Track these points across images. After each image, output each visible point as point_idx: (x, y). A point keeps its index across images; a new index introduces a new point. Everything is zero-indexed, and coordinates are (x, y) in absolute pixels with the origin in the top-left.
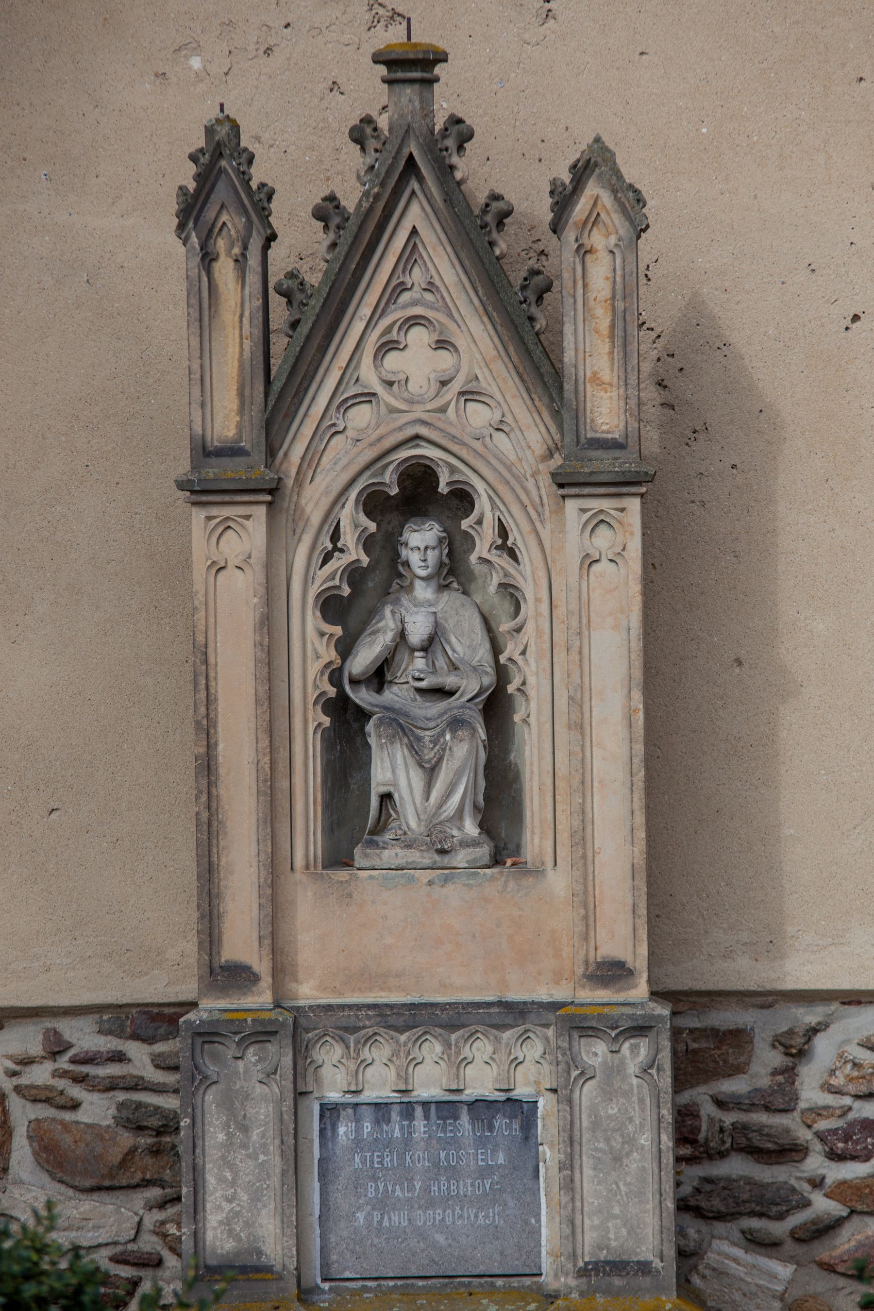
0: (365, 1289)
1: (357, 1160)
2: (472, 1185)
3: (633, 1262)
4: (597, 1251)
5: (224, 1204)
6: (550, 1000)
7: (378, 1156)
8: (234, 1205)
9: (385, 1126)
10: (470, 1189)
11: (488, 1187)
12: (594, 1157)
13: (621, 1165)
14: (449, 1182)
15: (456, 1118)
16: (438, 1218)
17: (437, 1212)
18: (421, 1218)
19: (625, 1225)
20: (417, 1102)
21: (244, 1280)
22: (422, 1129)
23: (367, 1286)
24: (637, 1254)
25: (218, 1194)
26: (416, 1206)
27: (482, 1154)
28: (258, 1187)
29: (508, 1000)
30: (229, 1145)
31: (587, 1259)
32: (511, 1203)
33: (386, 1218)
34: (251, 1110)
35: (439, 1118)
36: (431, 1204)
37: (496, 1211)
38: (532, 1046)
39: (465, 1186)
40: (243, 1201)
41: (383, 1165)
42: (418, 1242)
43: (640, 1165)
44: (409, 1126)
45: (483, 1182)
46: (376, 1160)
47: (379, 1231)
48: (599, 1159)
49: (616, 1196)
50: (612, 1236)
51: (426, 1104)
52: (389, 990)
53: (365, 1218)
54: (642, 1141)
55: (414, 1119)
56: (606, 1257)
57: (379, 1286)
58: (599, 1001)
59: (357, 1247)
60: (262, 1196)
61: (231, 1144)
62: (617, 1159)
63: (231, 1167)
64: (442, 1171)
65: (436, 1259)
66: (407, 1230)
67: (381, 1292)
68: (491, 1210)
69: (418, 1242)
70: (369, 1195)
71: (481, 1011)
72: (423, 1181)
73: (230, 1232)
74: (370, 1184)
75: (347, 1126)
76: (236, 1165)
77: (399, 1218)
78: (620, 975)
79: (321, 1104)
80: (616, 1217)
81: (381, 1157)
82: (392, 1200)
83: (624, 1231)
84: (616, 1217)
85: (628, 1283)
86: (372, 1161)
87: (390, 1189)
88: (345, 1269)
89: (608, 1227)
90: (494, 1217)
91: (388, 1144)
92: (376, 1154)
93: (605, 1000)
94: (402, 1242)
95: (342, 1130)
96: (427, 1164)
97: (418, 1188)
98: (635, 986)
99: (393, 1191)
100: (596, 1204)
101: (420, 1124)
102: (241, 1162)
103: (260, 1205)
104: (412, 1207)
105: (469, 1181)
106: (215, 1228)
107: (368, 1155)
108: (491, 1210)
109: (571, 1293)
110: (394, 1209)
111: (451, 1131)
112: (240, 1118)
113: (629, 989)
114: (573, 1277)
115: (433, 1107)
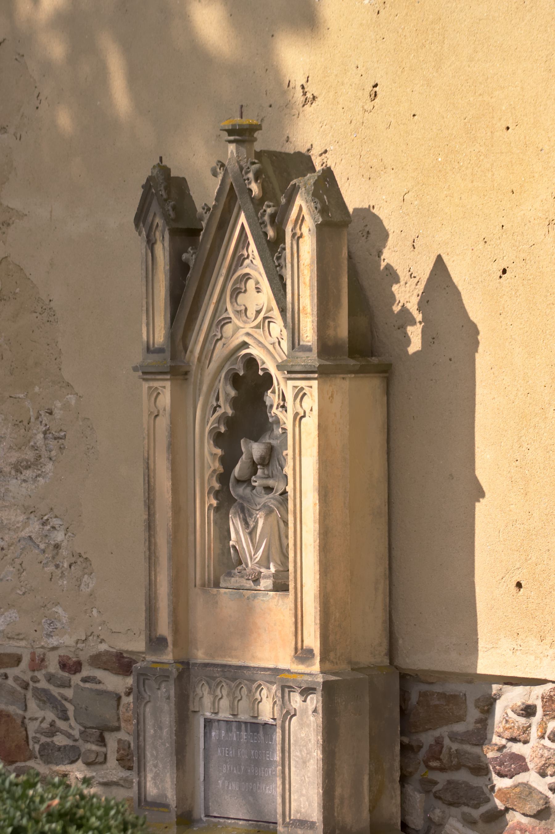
1: (219, 751)
3: (309, 821)
13: (306, 766)
14: (255, 768)
22: (245, 737)
50: (302, 806)
51: (246, 723)
56: (300, 817)
58: (300, 671)
86: (225, 753)
89: (300, 801)
93: (303, 671)
97: (242, 769)
98: (314, 664)
99: (233, 770)
111: (256, 740)
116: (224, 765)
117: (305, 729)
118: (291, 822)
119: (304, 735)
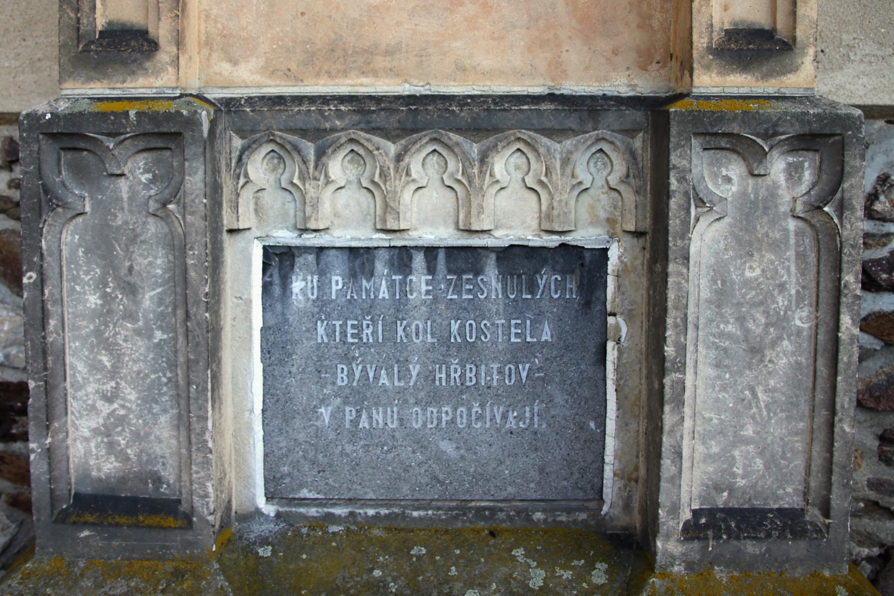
0: (331, 518)
1: (321, 330)
2: (500, 372)
3: (771, 510)
4: (713, 492)
5: (100, 404)
6: (631, 94)
7: (353, 326)
8: (116, 406)
9: (364, 282)
10: (496, 377)
11: (524, 375)
12: (717, 348)
13: (762, 361)
14: (463, 367)
15: (478, 272)
16: (444, 418)
17: (444, 409)
18: (418, 418)
19: (761, 454)
20: (416, 248)
21: (129, 526)
22: (424, 288)
23: (333, 515)
24: (777, 498)
25: (91, 388)
26: (412, 401)
27: (517, 326)
28: (153, 381)
29: (565, 92)
30: (105, 313)
31: (695, 506)
32: (559, 399)
33: (364, 416)
34: (140, 260)
35: (450, 271)
36: (435, 397)
37: (536, 410)
38: (604, 164)
39: (489, 373)
40: (130, 401)
41: (361, 339)
42: (414, 452)
43: (792, 359)
44: (403, 283)
45: (517, 368)
46: (350, 331)
47: (354, 434)
48: (725, 350)
49: (750, 408)
51: (430, 251)
52: (375, 74)
53: (332, 415)
54: (798, 323)
55: (410, 273)
56: (726, 502)
57: (352, 514)
58: (735, 91)
59: (320, 456)
60: (161, 395)
61: (110, 312)
62: (756, 351)
63: (110, 347)
64: (453, 351)
65: (441, 477)
66: (397, 434)
67: (355, 523)
68: (527, 409)
69: (414, 452)
70: (339, 383)
71: (526, 107)
72: (424, 365)
73: (111, 447)
74: (340, 366)
75: (305, 280)
76: (117, 344)
77: (385, 417)
78: (769, 50)
79: (265, 248)
80: (746, 441)
81: (359, 327)
82: (375, 391)
83: (759, 463)
84: (746, 441)
85: (768, 550)
86: (344, 334)
87: (371, 375)
88: (301, 486)
89: (733, 457)
90: (532, 419)
91: (371, 308)
92: (350, 323)
93: (743, 91)
94: (389, 451)
95: (297, 285)
96: (430, 339)
97: (414, 373)
98: (794, 69)
99: (377, 378)
100: (715, 421)
101: (420, 280)
102: (125, 341)
103: (156, 409)
104: (406, 401)
105: (495, 366)
106: (87, 440)
107: (338, 323)
108: (527, 409)
109: (672, 565)
110: (377, 405)
111: (469, 291)
112: (124, 271)
113: (784, 74)
114: (679, 541)
115: (441, 256)
116: (340, 366)
117: (762, 256)
118: (703, 521)
119: (758, 272)
